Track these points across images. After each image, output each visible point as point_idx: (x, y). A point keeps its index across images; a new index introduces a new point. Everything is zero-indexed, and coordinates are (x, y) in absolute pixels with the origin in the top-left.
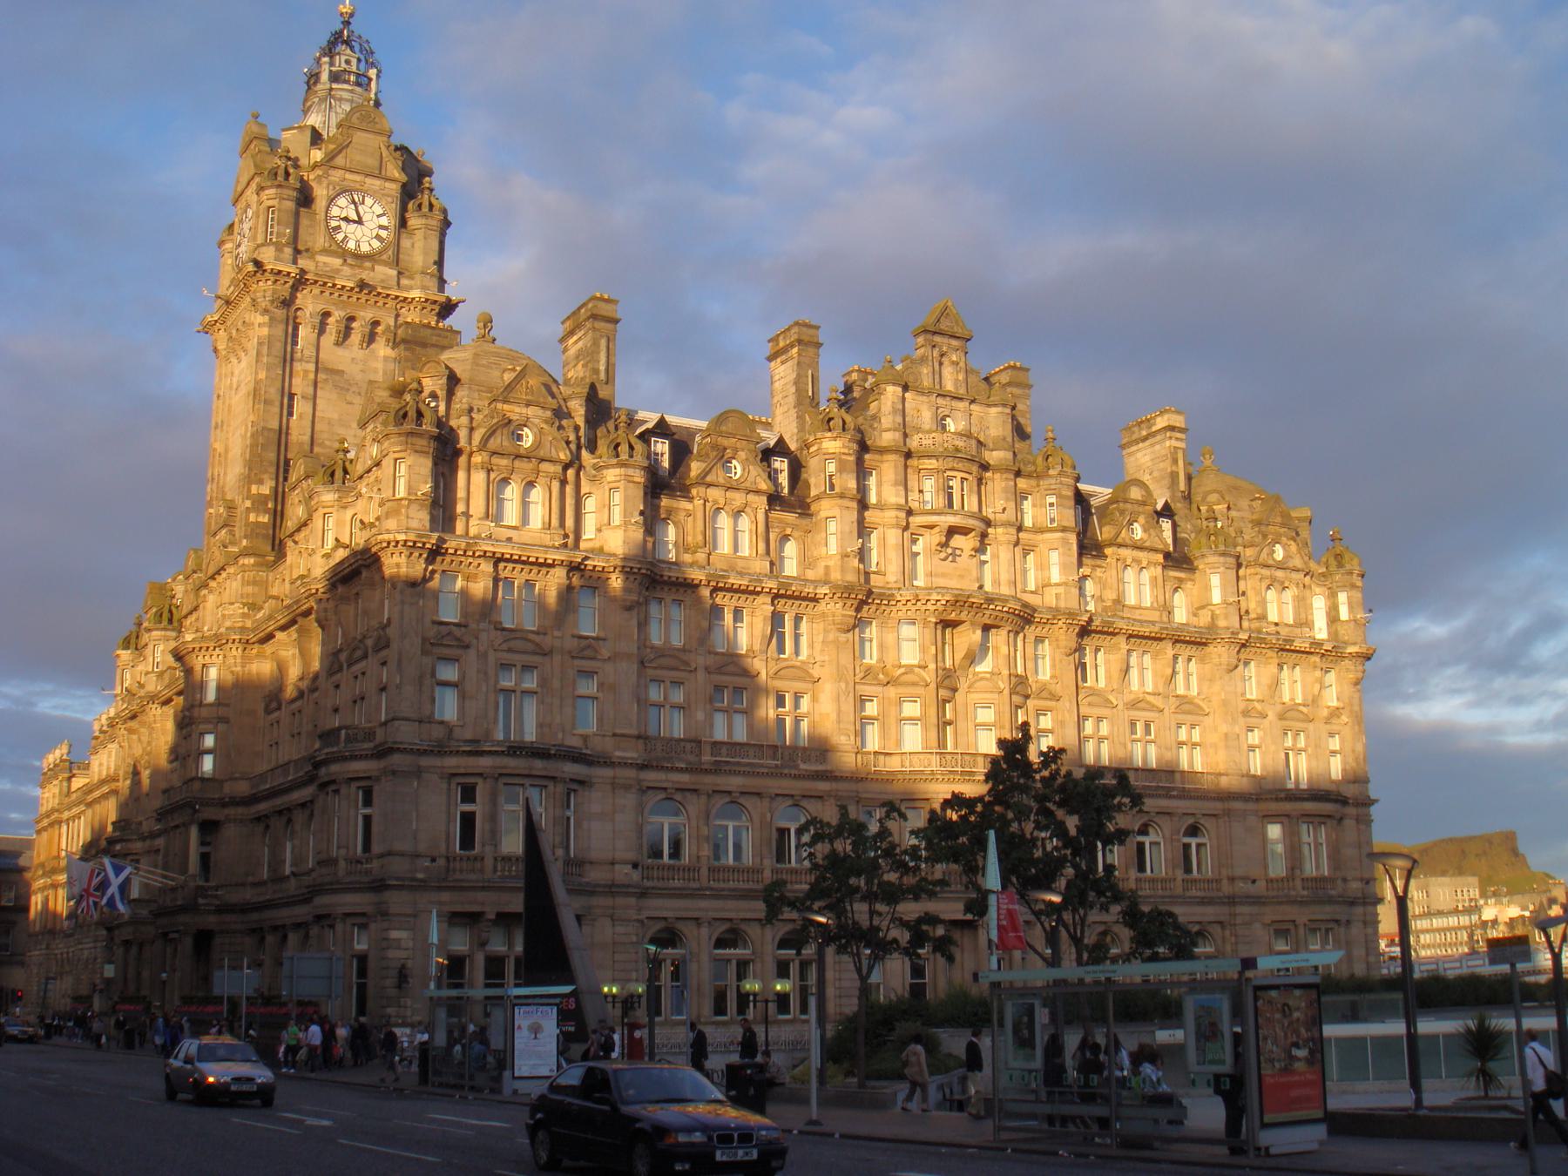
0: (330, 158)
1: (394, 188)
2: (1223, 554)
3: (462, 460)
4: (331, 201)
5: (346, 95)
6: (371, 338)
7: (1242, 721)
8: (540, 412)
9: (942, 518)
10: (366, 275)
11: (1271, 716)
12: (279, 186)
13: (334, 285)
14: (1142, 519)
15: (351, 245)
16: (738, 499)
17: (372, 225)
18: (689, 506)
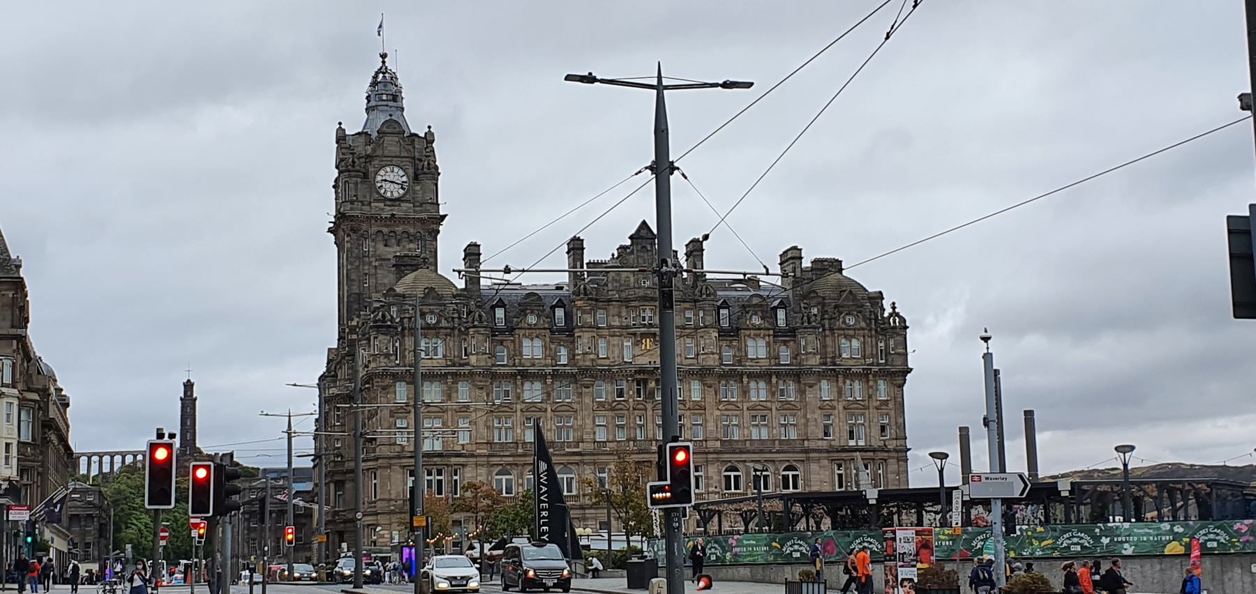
4: (376, 173)
7: (819, 412)
11: (841, 408)
15: (389, 194)
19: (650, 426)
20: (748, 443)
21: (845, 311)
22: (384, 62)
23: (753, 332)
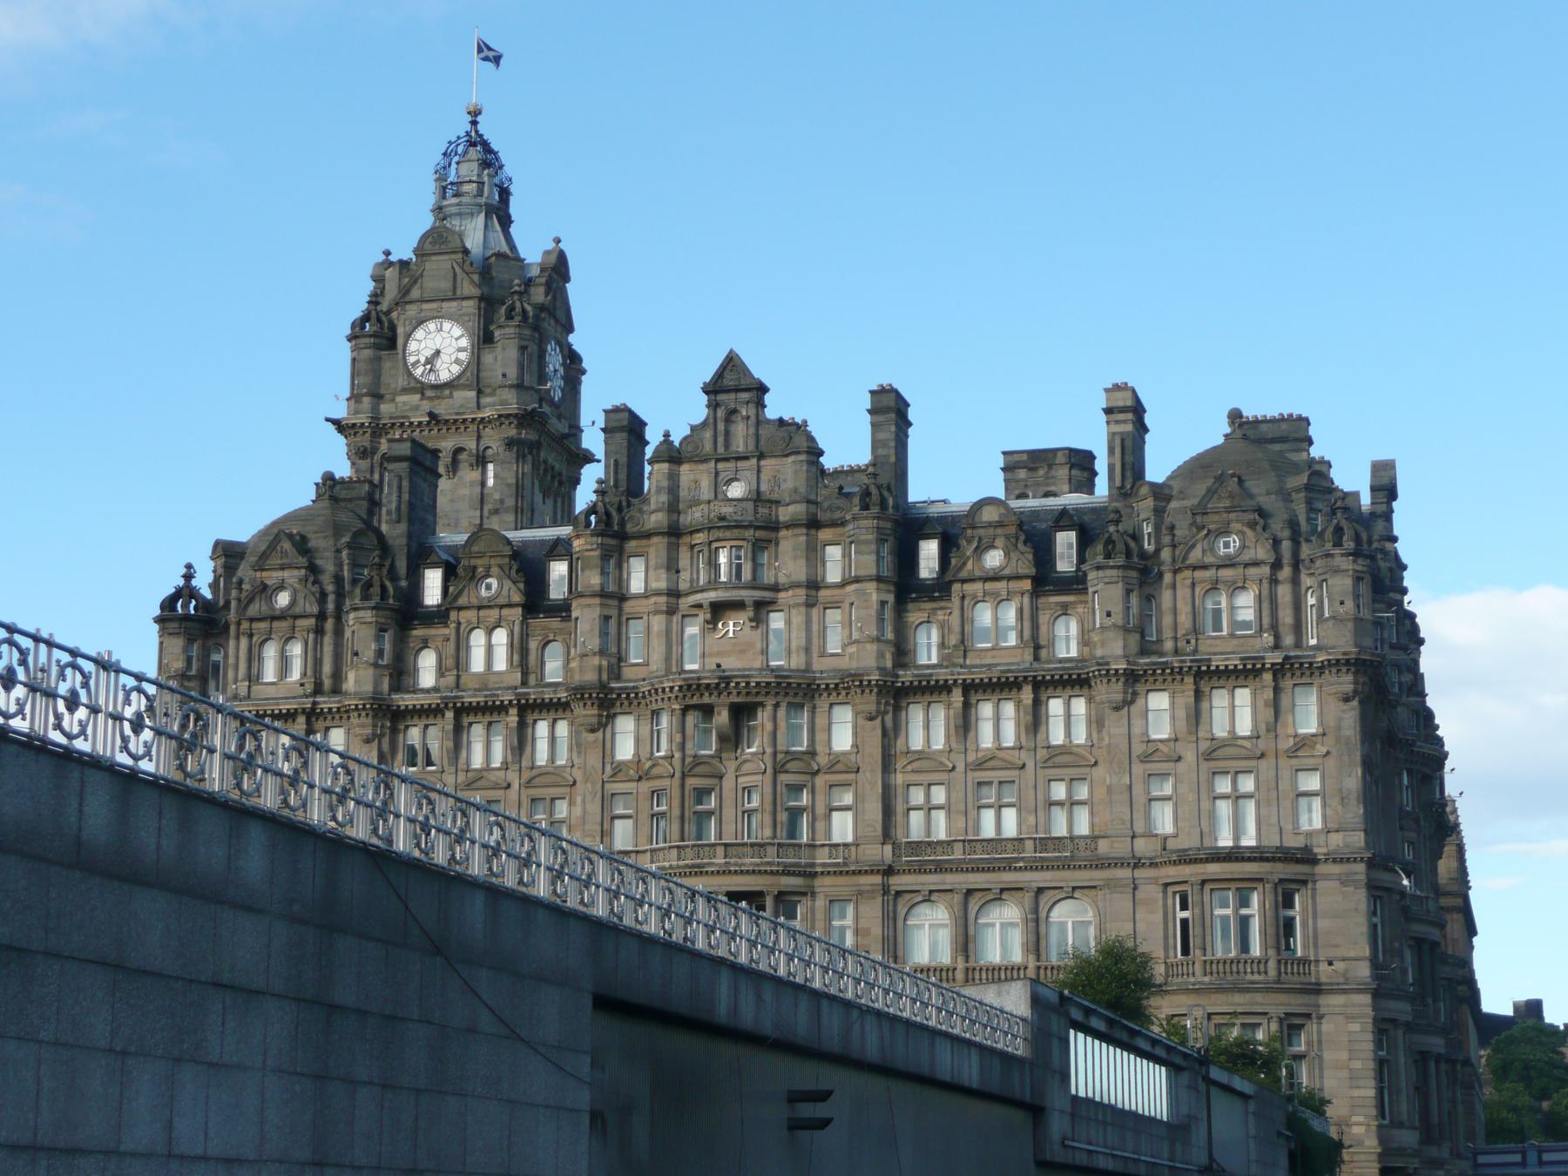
2: (1098, 568)
3: (233, 628)
4: (408, 336)
7: (1138, 769)
8: (296, 572)
9: (705, 595)
11: (1190, 756)
14: (999, 542)
16: (493, 614)
17: (451, 350)
18: (446, 631)
19: (729, 813)
20: (958, 847)
21: (1213, 522)
22: (474, 123)
23: (978, 586)
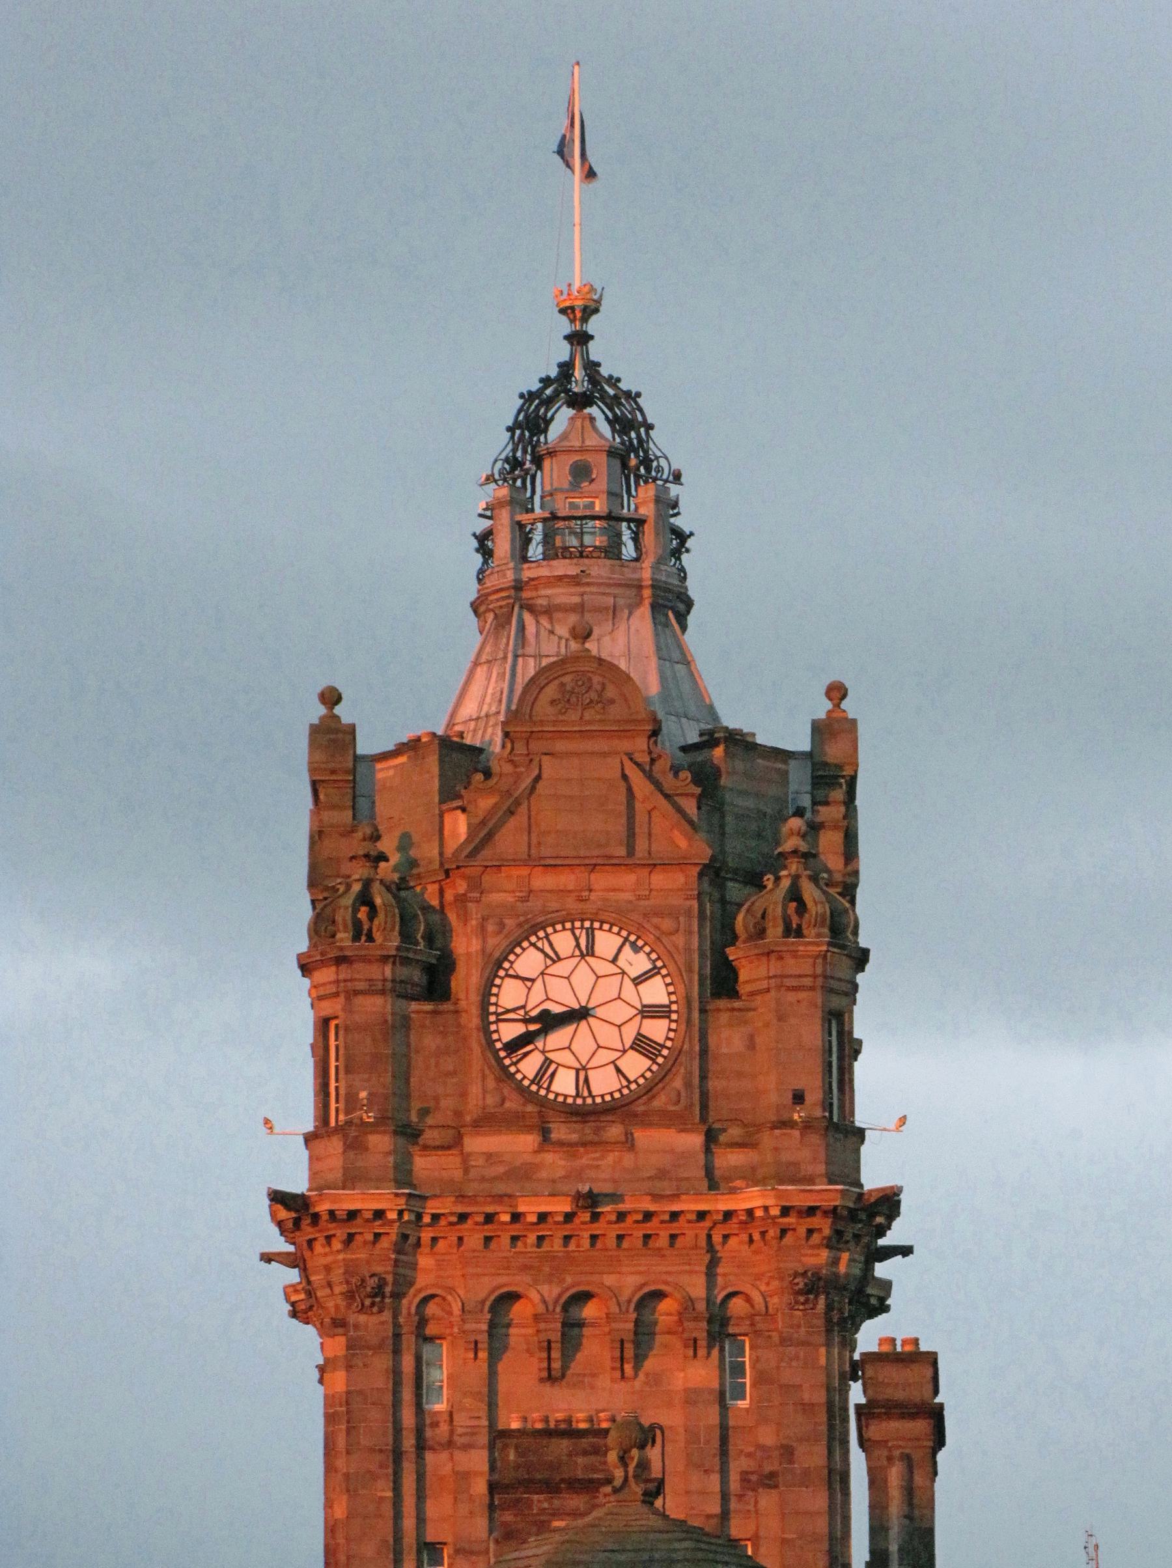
0: (484, 836)
1: (675, 887)
4: (496, 967)
5: (563, 595)
6: (640, 1340)
10: (603, 1170)
12: (340, 960)
13: (516, 1217)
15: (564, 1084)
17: (619, 1012)
22: (580, 339)
